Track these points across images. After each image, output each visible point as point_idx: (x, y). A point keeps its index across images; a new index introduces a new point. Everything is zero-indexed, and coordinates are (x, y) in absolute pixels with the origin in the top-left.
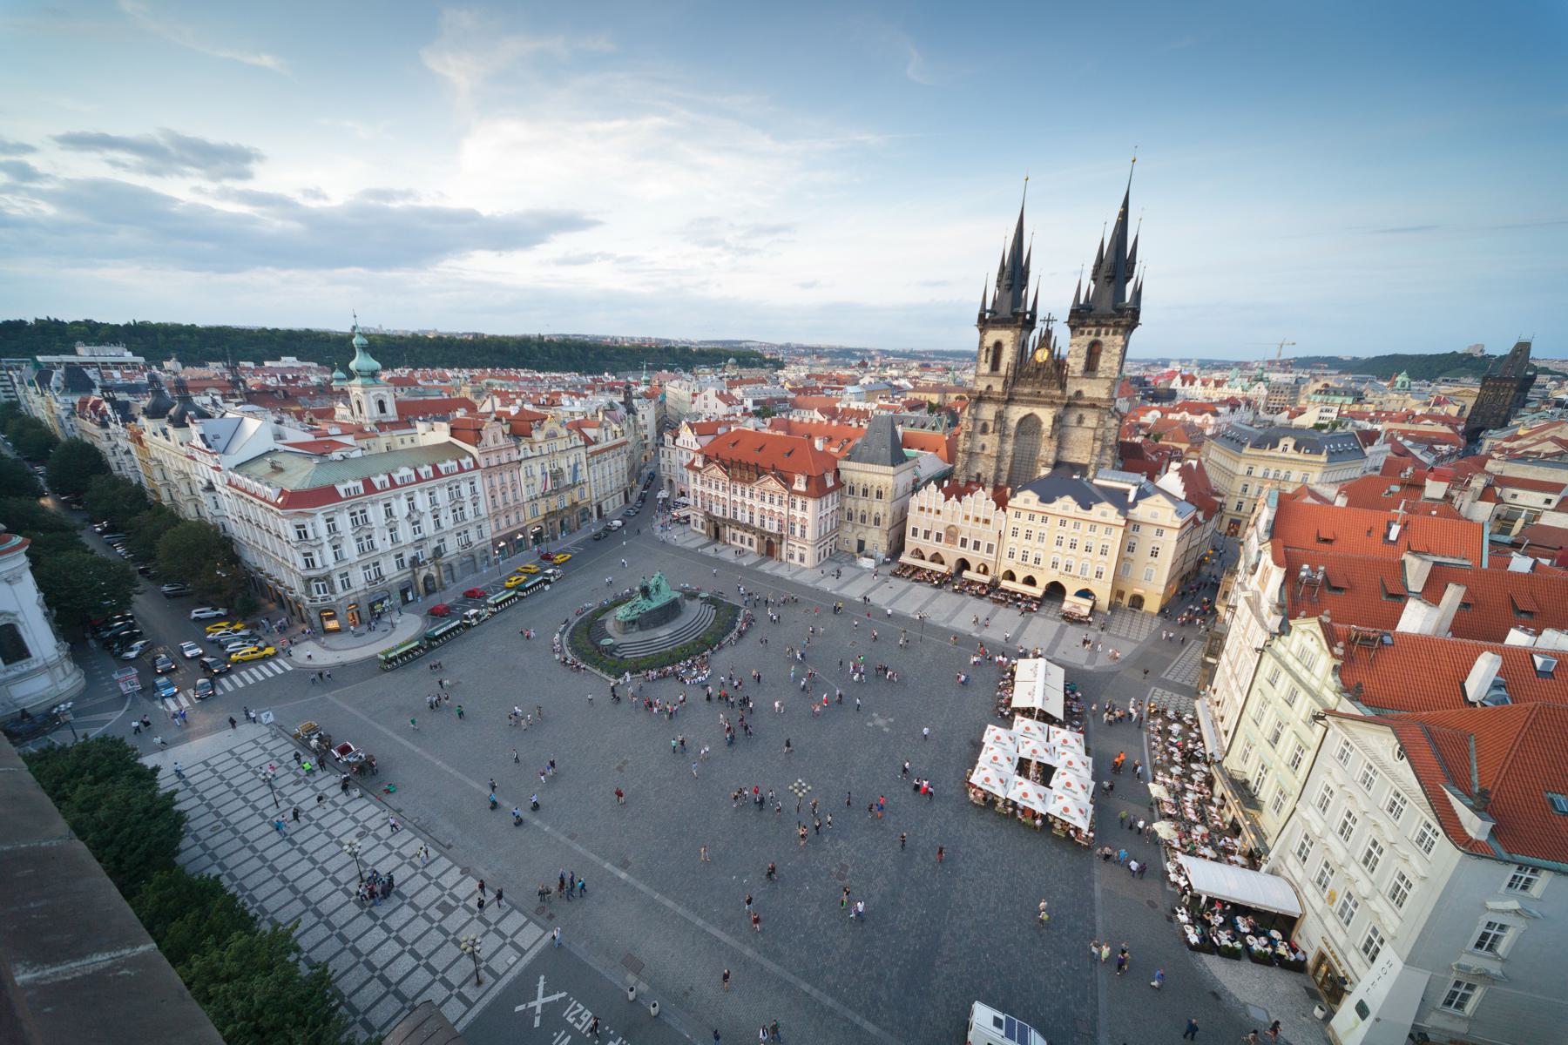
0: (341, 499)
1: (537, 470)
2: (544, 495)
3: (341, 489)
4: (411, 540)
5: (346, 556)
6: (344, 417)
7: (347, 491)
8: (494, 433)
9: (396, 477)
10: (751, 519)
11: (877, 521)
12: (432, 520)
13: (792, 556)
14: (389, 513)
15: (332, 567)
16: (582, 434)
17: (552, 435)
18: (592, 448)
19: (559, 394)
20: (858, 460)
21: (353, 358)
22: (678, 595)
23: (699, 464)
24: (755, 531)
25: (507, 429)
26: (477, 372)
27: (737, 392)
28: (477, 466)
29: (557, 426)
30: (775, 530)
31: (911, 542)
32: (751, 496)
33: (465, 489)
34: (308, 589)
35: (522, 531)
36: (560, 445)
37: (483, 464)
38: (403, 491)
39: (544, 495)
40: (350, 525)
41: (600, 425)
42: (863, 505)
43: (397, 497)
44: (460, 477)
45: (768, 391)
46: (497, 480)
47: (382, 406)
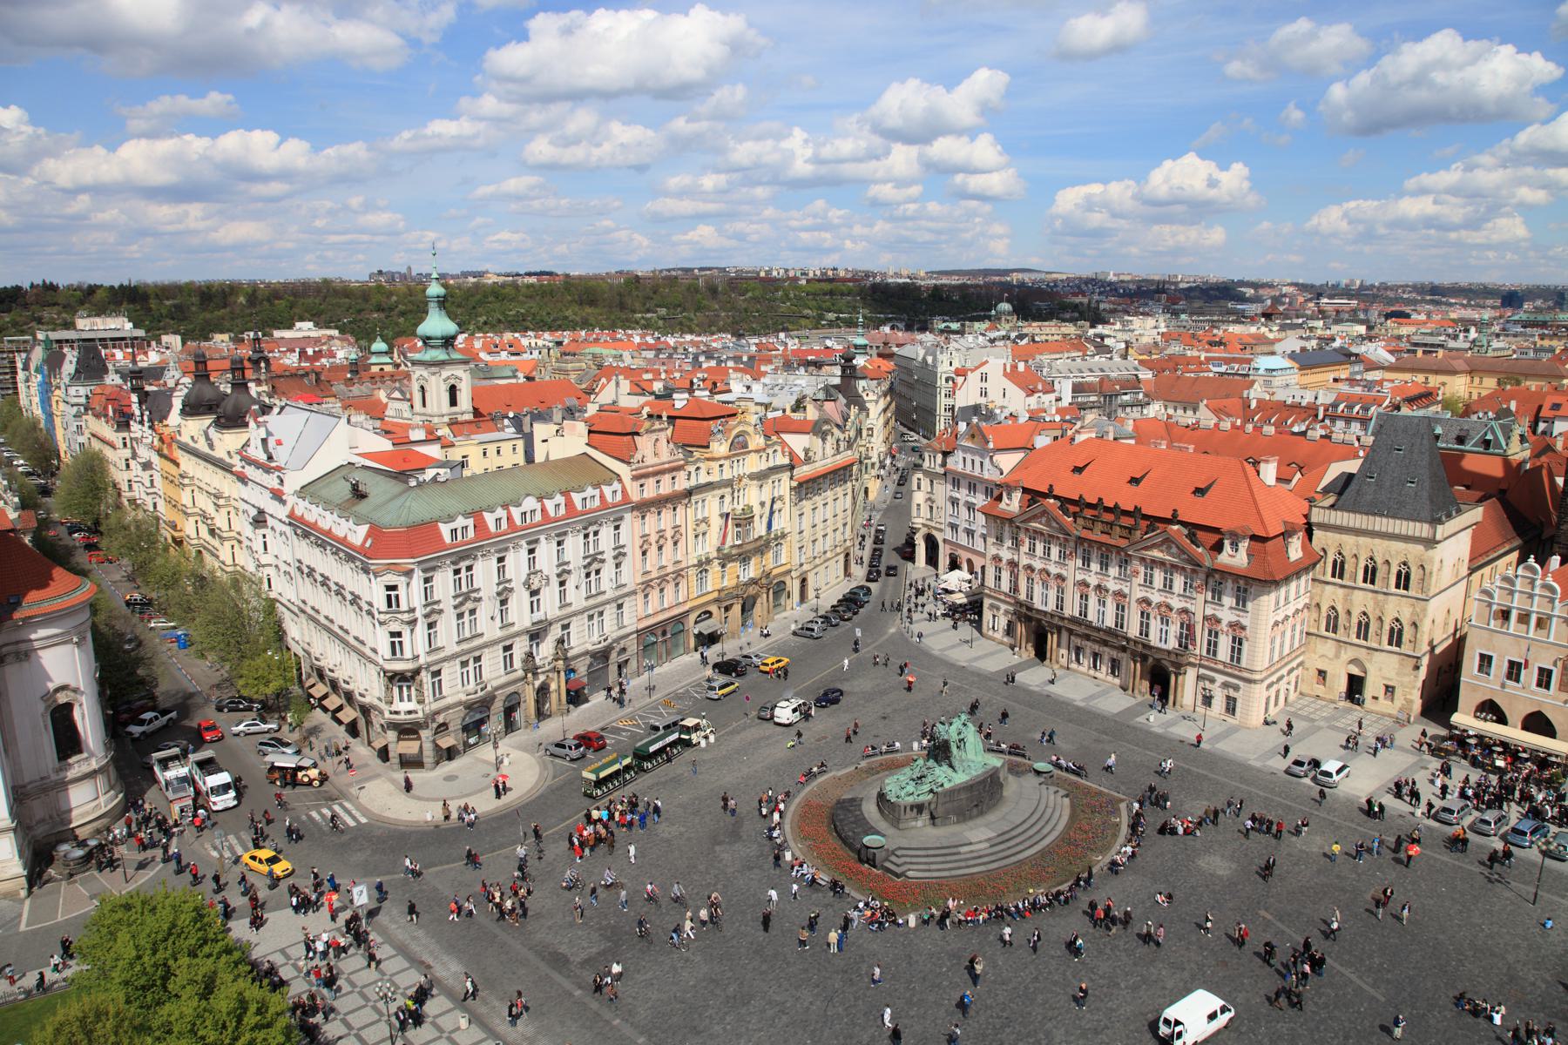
3: (445, 530)
10: (1120, 621)
11: (1396, 637)
12: (557, 588)
13: (1208, 701)
15: (422, 660)
16: (784, 444)
17: (739, 446)
20: (1354, 509)
23: (1013, 504)
26: (566, 337)
29: (750, 429)
30: (1172, 644)
31: (1473, 686)
42: (1362, 601)
47: (453, 390)
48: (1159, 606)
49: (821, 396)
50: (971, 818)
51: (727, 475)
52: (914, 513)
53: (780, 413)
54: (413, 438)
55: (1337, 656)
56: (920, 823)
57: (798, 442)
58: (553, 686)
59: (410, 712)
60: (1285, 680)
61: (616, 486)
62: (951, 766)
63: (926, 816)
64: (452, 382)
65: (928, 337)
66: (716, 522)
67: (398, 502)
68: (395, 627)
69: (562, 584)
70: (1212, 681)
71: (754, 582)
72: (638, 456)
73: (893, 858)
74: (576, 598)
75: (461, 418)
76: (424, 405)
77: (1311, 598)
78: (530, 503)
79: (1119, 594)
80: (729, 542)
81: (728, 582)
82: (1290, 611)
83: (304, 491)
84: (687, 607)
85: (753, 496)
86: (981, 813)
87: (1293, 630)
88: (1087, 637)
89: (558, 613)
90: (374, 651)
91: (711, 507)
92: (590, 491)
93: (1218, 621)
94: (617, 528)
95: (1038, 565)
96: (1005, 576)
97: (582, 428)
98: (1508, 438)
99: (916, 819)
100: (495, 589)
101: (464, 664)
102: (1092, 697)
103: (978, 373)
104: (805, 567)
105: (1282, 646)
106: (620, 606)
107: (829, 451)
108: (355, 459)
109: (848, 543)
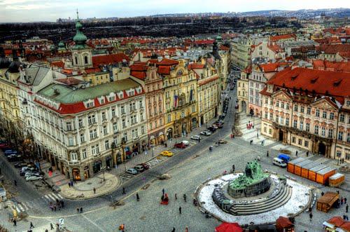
1: (172, 95)
2: (175, 110)
3: (85, 103)
4: (112, 133)
5: (86, 140)
6: (69, 66)
8: (152, 73)
9: (108, 97)
15: (80, 146)
16: (195, 72)
17: (180, 74)
18: (201, 81)
19: (174, 49)
21: (75, 35)
23: (270, 90)
24: (310, 136)
26: (122, 39)
27: (281, 42)
30: (327, 136)
32: (309, 113)
33: (137, 104)
34: (69, 156)
35: (163, 130)
36: (183, 79)
37: (146, 91)
40: (88, 124)
41: (204, 67)
45: (301, 41)
46: (152, 99)
47: (86, 58)
48: (322, 123)
49: (206, 56)
57: (199, 72)
61: (140, 88)
62: (251, 177)
63: (243, 194)
65: (242, 35)
67: (70, 95)
69: (123, 120)
70: (341, 148)
71: (185, 118)
72: (147, 78)
75: (89, 67)
76: (77, 63)
78: (112, 95)
79: (308, 119)
80: (177, 106)
81: (178, 119)
83: (39, 92)
85: (184, 90)
90: (64, 143)
92: (131, 90)
93: (343, 128)
96: (269, 114)
97: (128, 69)
101: (93, 147)
103: (258, 47)
106: (143, 127)
108: (55, 82)
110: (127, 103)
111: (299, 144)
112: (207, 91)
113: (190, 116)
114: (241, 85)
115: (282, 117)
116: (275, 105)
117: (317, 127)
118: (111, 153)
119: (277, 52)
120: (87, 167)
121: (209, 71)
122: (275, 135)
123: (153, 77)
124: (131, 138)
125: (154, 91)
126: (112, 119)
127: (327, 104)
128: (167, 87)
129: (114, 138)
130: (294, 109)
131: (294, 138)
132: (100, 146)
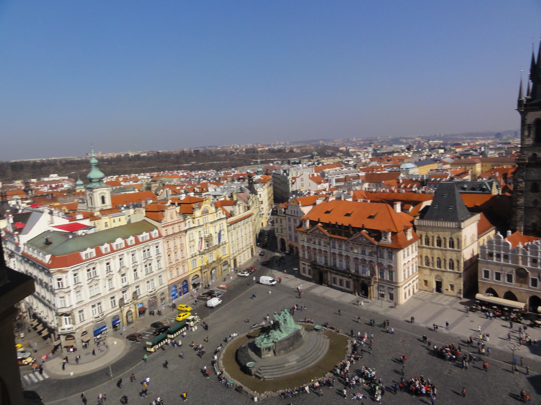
0: (83, 261)
3: (83, 254)
4: (120, 287)
7: (86, 255)
8: (172, 214)
11: (452, 266)
12: (133, 273)
14: (109, 270)
15: (74, 307)
17: (206, 212)
20: (430, 218)
22: (299, 327)
25: (178, 209)
26: (155, 174)
28: (160, 236)
29: (209, 206)
33: (153, 250)
34: (60, 321)
38: (117, 255)
39: (201, 254)
40: (86, 278)
43: (114, 258)
44: (150, 243)
46: (171, 243)
47: (103, 198)
48: (362, 260)
49: (239, 191)
50: (290, 351)
51: (201, 224)
52: (276, 231)
53: (223, 199)
54: (78, 218)
55: (430, 275)
56: (270, 355)
57: (228, 209)
58: (133, 310)
59: (69, 329)
60: (411, 285)
61: (156, 231)
62: (280, 331)
64: (103, 195)
66: (197, 240)
68: (62, 295)
69: (135, 270)
71: (214, 262)
72: (164, 220)
73: (259, 371)
74: (141, 274)
75: (105, 208)
76: (92, 204)
77: (418, 253)
78: (119, 241)
82: (410, 258)
83: (30, 243)
84: (188, 274)
85: (213, 231)
86: (294, 349)
87: (412, 265)
88: (337, 274)
89: (134, 282)
90: (54, 305)
91: (195, 235)
94: (157, 247)
95: (317, 247)
96: (306, 252)
98: (491, 187)
99: (268, 354)
100: (105, 275)
102: (340, 297)
103: (299, 178)
104: (235, 255)
105: (408, 272)
107: (242, 211)
109: (252, 244)
110: (139, 250)
111: (341, 285)
112: (239, 229)
113: (219, 259)
114: (279, 221)
115: (320, 256)
116: (312, 242)
117: (357, 265)
118: (119, 311)
119: (319, 183)
120: (85, 333)
121: (241, 207)
122: (314, 275)
123: (172, 218)
124: (144, 291)
125: (174, 234)
126: (120, 271)
127: (364, 239)
128: (190, 229)
129: (123, 292)
130: (331, 247)
131: (334, 278)
132: (103, 305)
